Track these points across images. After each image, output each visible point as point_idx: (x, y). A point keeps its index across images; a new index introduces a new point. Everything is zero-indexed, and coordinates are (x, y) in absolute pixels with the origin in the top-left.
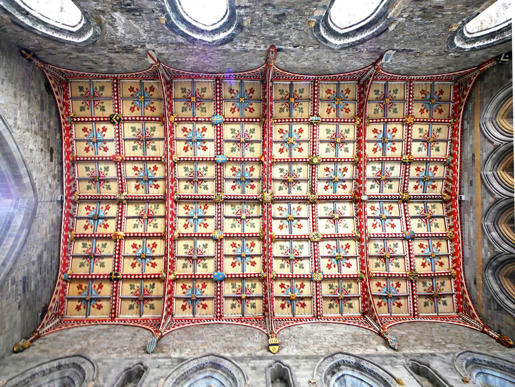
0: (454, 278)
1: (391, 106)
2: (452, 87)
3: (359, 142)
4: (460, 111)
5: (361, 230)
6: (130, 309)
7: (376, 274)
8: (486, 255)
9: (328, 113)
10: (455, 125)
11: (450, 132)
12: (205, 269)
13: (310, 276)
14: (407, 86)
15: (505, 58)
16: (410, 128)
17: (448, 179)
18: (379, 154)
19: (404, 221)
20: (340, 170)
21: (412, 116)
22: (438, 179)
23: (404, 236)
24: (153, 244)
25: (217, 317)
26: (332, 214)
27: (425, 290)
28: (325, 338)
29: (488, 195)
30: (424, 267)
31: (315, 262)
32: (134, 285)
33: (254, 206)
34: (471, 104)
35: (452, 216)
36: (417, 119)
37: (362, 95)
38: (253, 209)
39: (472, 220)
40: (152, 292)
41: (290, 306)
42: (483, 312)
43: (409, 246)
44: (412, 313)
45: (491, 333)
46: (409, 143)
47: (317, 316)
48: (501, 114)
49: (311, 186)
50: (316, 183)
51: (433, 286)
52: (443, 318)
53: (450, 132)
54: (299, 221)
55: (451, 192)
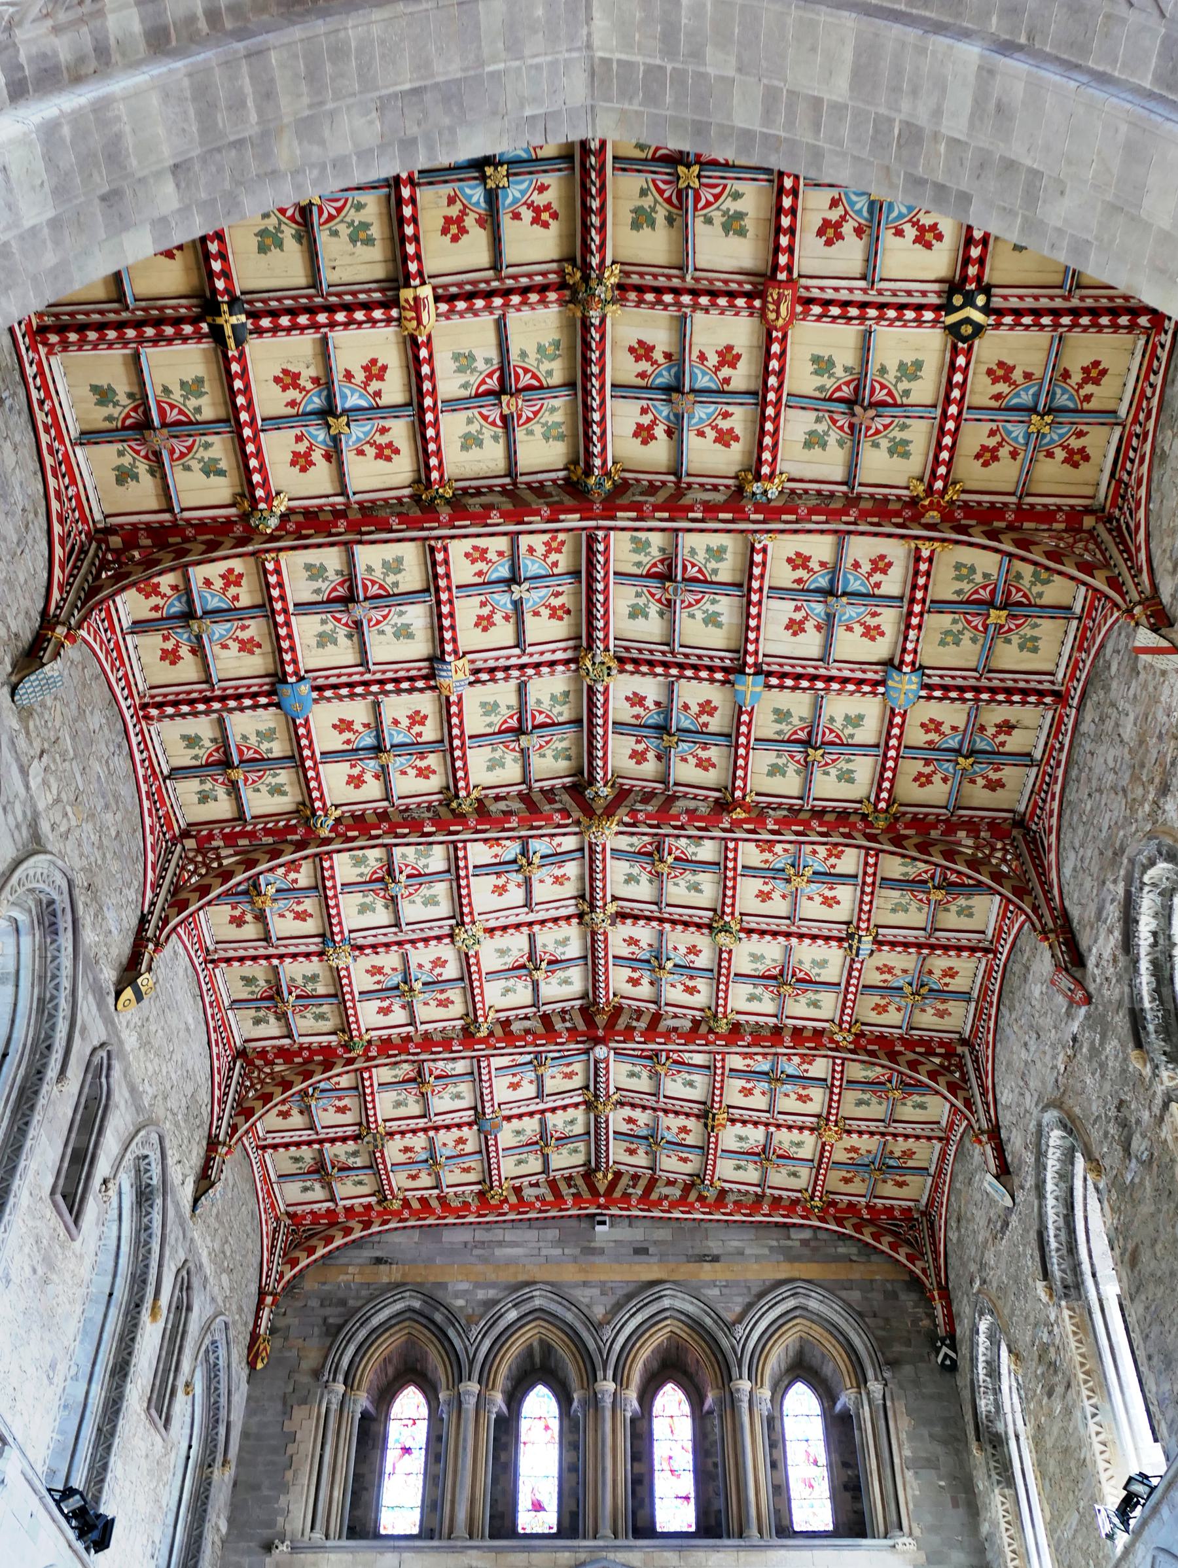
0: (379, 1202)
2: (911, 1204)
6: (95, 389)
8: (457, 1295)
10: (805, 1209)
11: (784, 1194)
12: (313, 642)
15: (946, 1356)
17: (652, 1182)
19: (533, 1108)
25: (144, 706)
29: (610, 1300)
32: (201, 394)
33: (569, 758)
34: (854, 1250)
35: (550, 1198)
38: (555, 758)
39: (544, 1252)
40: (188, 468)
42: (309, 1285)
44: (269, 1141)
47: (212, 961)
53: (784, 1194)
55: (617, 1194)
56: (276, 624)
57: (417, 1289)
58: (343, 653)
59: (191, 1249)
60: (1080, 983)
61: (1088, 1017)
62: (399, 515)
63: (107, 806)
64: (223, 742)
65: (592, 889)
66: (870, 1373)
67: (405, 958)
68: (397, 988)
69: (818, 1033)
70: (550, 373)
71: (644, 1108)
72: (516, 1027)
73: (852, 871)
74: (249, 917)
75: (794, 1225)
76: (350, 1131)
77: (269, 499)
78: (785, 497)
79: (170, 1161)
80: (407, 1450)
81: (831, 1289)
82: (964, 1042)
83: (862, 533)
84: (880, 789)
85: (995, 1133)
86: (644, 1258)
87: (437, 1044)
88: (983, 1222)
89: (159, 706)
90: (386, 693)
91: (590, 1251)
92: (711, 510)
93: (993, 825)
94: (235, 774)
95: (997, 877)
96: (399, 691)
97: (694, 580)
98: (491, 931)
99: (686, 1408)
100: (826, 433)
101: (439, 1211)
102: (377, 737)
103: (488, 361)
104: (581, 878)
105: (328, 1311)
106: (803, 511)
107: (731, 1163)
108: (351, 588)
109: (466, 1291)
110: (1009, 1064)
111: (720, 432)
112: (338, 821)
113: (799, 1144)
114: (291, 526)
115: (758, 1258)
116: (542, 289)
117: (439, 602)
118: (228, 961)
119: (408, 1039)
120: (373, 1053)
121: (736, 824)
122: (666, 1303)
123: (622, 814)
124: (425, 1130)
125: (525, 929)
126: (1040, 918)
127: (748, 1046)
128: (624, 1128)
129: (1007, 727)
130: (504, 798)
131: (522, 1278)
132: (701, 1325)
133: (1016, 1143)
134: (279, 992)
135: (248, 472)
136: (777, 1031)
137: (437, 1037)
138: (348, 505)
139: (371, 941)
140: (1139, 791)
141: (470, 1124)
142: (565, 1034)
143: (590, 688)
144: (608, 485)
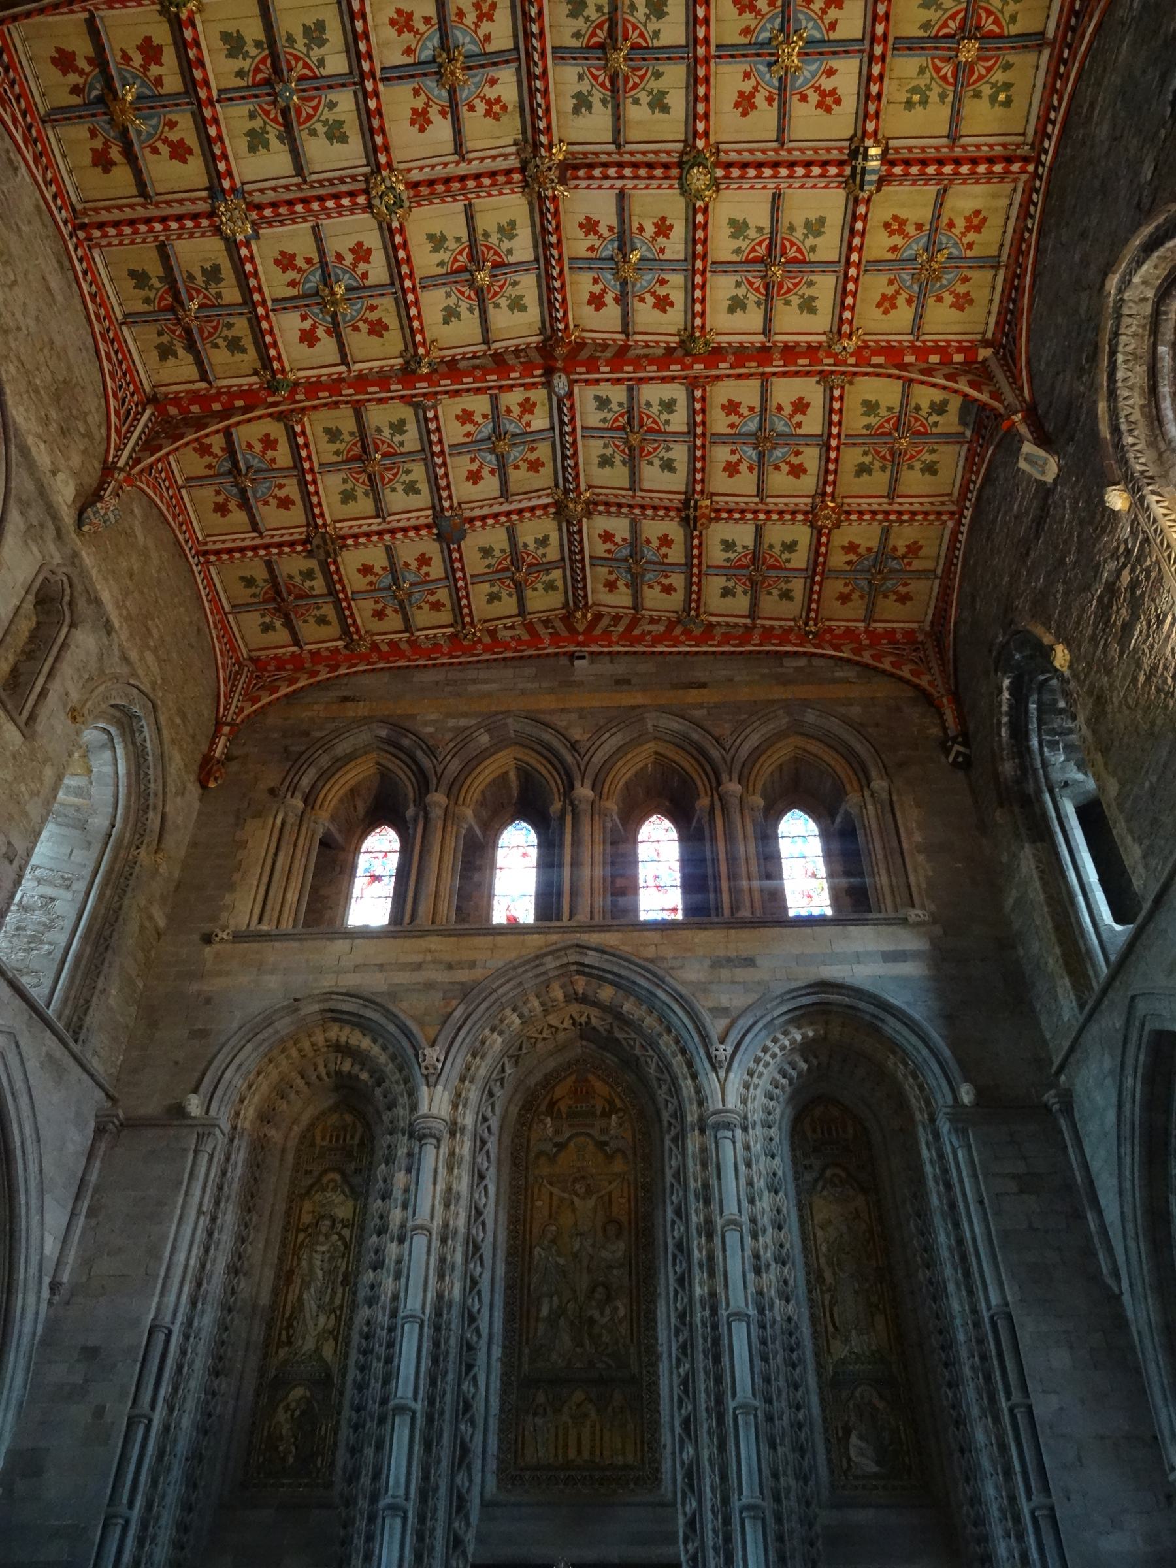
0: (346, 647)
1: (884, 458)
3: (764, 353)
4: (837, 648)
5: (444, 377)
7: (303, 433)
8: (426, 724)
9: (887, 225)
13: (226, 184)
14: (943, 503)
16: (800, 517)
17: (635, 622)
18: (720, 422)
19: (496, 509)
20: (663, 282)
21: (838, 525)
22: (637, 597)
23: (447, 514)
26: (490, 255)
27: (290, 577)
28: (15, 283)
30: (359, 571)
31: (290, 203)
35: (526, 637)
36: (828, 535)
37: (934, 359)
39: (520, 686)
41: (76, 100)
43: (417, 528)
44: (210, 547)
46: (750, 516)
47: (83, 227)
48: (809, 747)
49: (591, 159)
50: (607, 184)
51: (308, 596)
52: (224, 628)
54: (443, 113)
55: (598, 631)
57: (384, 721)
66: (874, 773)
72: (462, 365)
75: (787, 652)
80: (375, 878)
86: (625, 687)
99: (674, 834)
109: (436, 721)
119: (341, 380)
127: (732, 367)
142: (519, 368)
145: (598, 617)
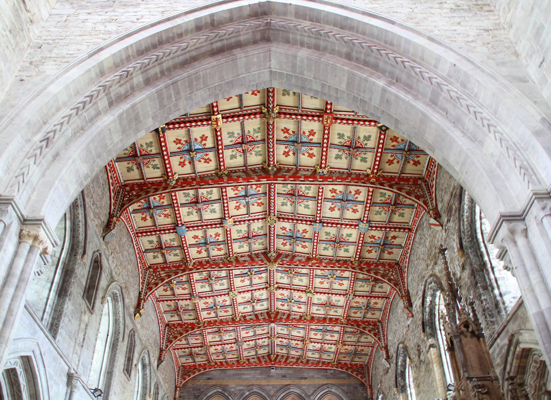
0: (208, 363)
4: (342, 368)
8: (232, 388)
12: (186, 214)
17: (288, 358)
19: (252, 339)
24: (209, 159)
25: (137, 233)
29: (275, 389)
34: (346, 376)
35: (258, 362)
38: (259, 245)
42: (189, 385)
45: (178, 392)
53: (326, 361)
55: (277, 361)
56: (175, 210)
57: (221, 386)
58: (195, 217)
59: (158, 379)
60: (411, 312)
61: (412, 321)
62: (212, 179)
63: (129, 264)
64: (160, 242)
65: (270, 281)
67: (215, 300)
68: (212, 307)
69: (337, 320)
70: (257, 137)
71: (285, 338)
72: (248, 318)
73: (348, 276)
74: (169, 289)
76: (199, 345)
77: (173, 175)
78: (329, 173)
79: (151, 357)
81: (338, 386)
82: (379, 322)
83: (352, 185)
84: (356, 255)
85: (386, 348)
87: (224, 323)
88: (382, 370)
89: (141, 233)
90: (208, 228)
91: (270, 376)
92: (306, 177)
93: (389, 265)
94: (163, 251)
95: (390, 280)
96: (212, 228)
97: (302, 196)
98: (240, 292)
100: (342, 155)
101: (225, 365)
102: (205, 240)
103: (238, 134)
104: (267, 277)
105: (195, 392)
106: (334, 178)
107: (311, 353)
108: (197, 199)
110: (391, 329)
111: (309, 154)
112: (194, 263)
113: (331, 348)
114: (179, 183)
115: (318, 378)
116: (255, 114)
117: (224, 203)
118: (163, 301)
119: (216, 321)
120: (206, 325)
121: (314, 264)
122: (291, 390)
123: (279, 261)
124: (221, 345)
125: (250, 292)
126: (401, 292)
128: (279, 343)
129: (394, 237)
130: (243, 256)
131: (250, 383)
132: (301, 396)
133: (392, 351)
134: (178, 309)
135: (166, 169)
136: (325, 319)
137: (224, 321)
138: (196, 176)
139: (205, 295)
140: (429, 262)
141: (234, 343)
142: (262, 320)
143: (269, 226)
144: (275, 169)
145: (278, 356)
